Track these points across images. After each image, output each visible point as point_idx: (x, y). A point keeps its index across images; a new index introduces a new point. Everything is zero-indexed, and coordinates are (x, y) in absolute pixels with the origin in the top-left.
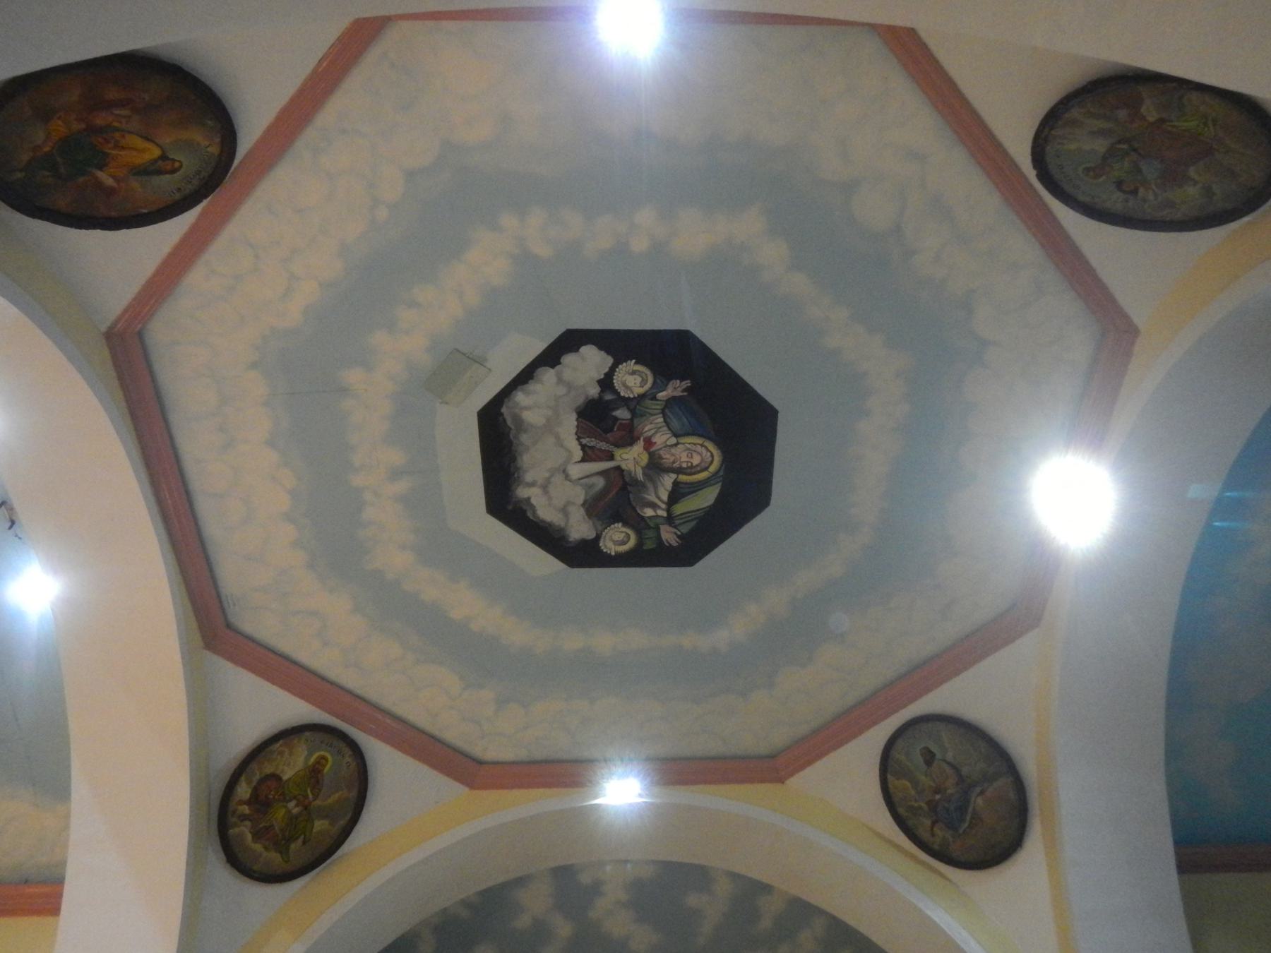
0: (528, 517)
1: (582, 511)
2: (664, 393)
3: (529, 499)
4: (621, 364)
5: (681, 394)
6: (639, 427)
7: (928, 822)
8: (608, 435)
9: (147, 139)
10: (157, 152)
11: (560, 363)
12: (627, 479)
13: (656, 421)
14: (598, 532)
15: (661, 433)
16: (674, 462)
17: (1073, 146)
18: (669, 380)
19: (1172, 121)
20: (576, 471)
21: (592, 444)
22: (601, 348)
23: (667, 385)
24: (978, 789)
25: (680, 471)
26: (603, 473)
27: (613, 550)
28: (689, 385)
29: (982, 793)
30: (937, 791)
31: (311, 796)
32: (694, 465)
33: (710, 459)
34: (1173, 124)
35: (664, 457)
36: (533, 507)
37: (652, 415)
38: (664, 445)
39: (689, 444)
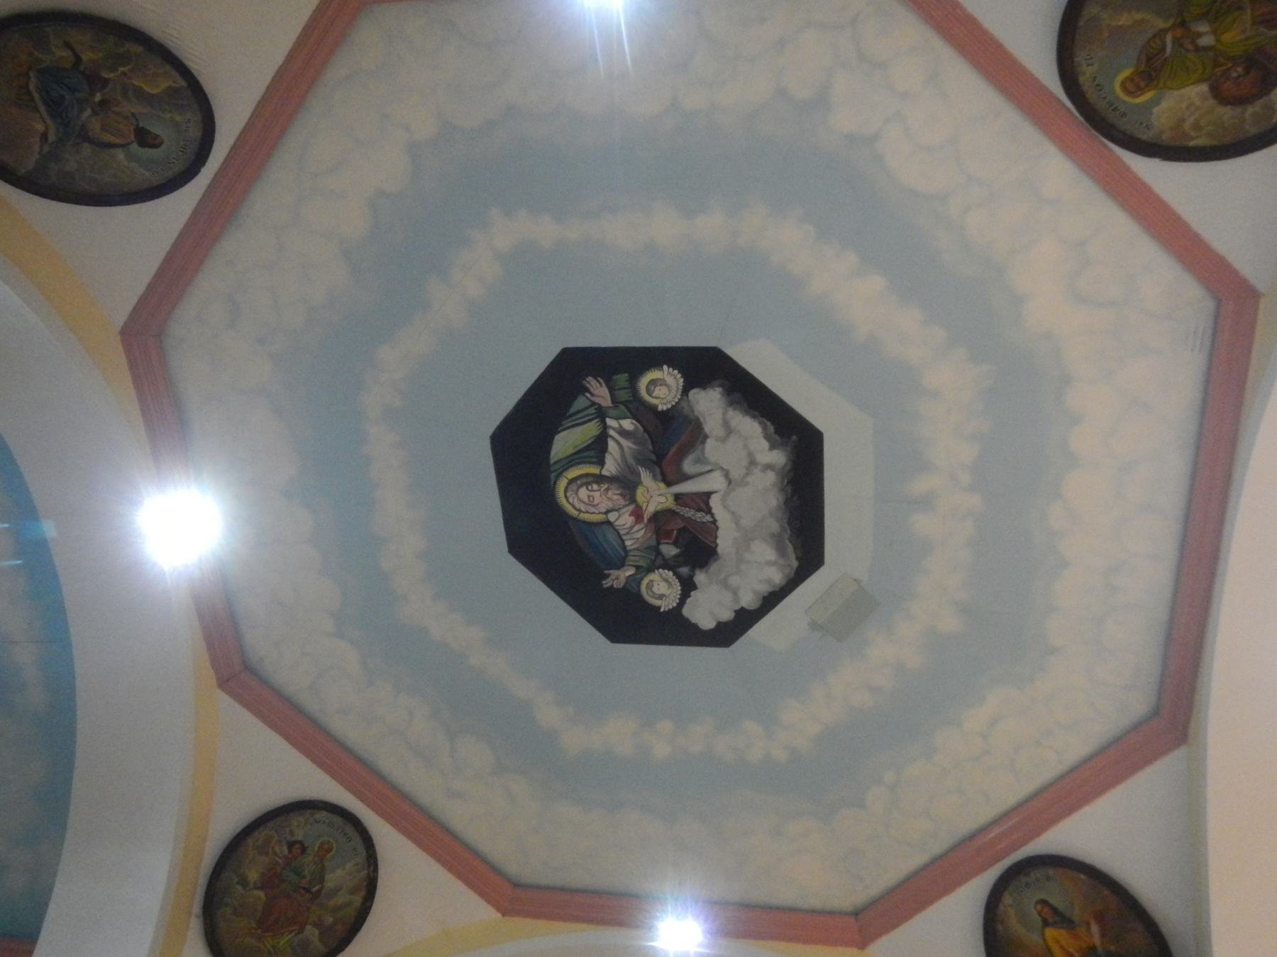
0: (773, 423)
1: (707, 429)
2: (628, 574)
3: (772, 447)
4: (674, 608)
5: (611, 572)
6: (649, 535)
7: (87, 56)
8: (682, 525)
9: (1049, 949)
10: (1050, 933)
11: (736, 611)
12: (658, 470)
13: (635, 540)
14: (685, 398)
15: (626, 527)
16: (607, 489)
17: (348, 866)
18: (624, 588)
19: (296, 935)
20: (714, 482)
21: (699, 515)
22: (695, 626)
23: (626, 583)
24: (52, 137)
25: (600, 479)
26: (687, 478)
27: (666, 372)
28: (604, 582)
29: (44, 137)
30: (104, 103)
31: (1169, 38)
32: (584, 488)
33: (568, 494)
34: (293, 934)
35: (619, 497)
36: (767, 437)
37: (637, 549)
38: (622, 511)
39: (593, 513)
